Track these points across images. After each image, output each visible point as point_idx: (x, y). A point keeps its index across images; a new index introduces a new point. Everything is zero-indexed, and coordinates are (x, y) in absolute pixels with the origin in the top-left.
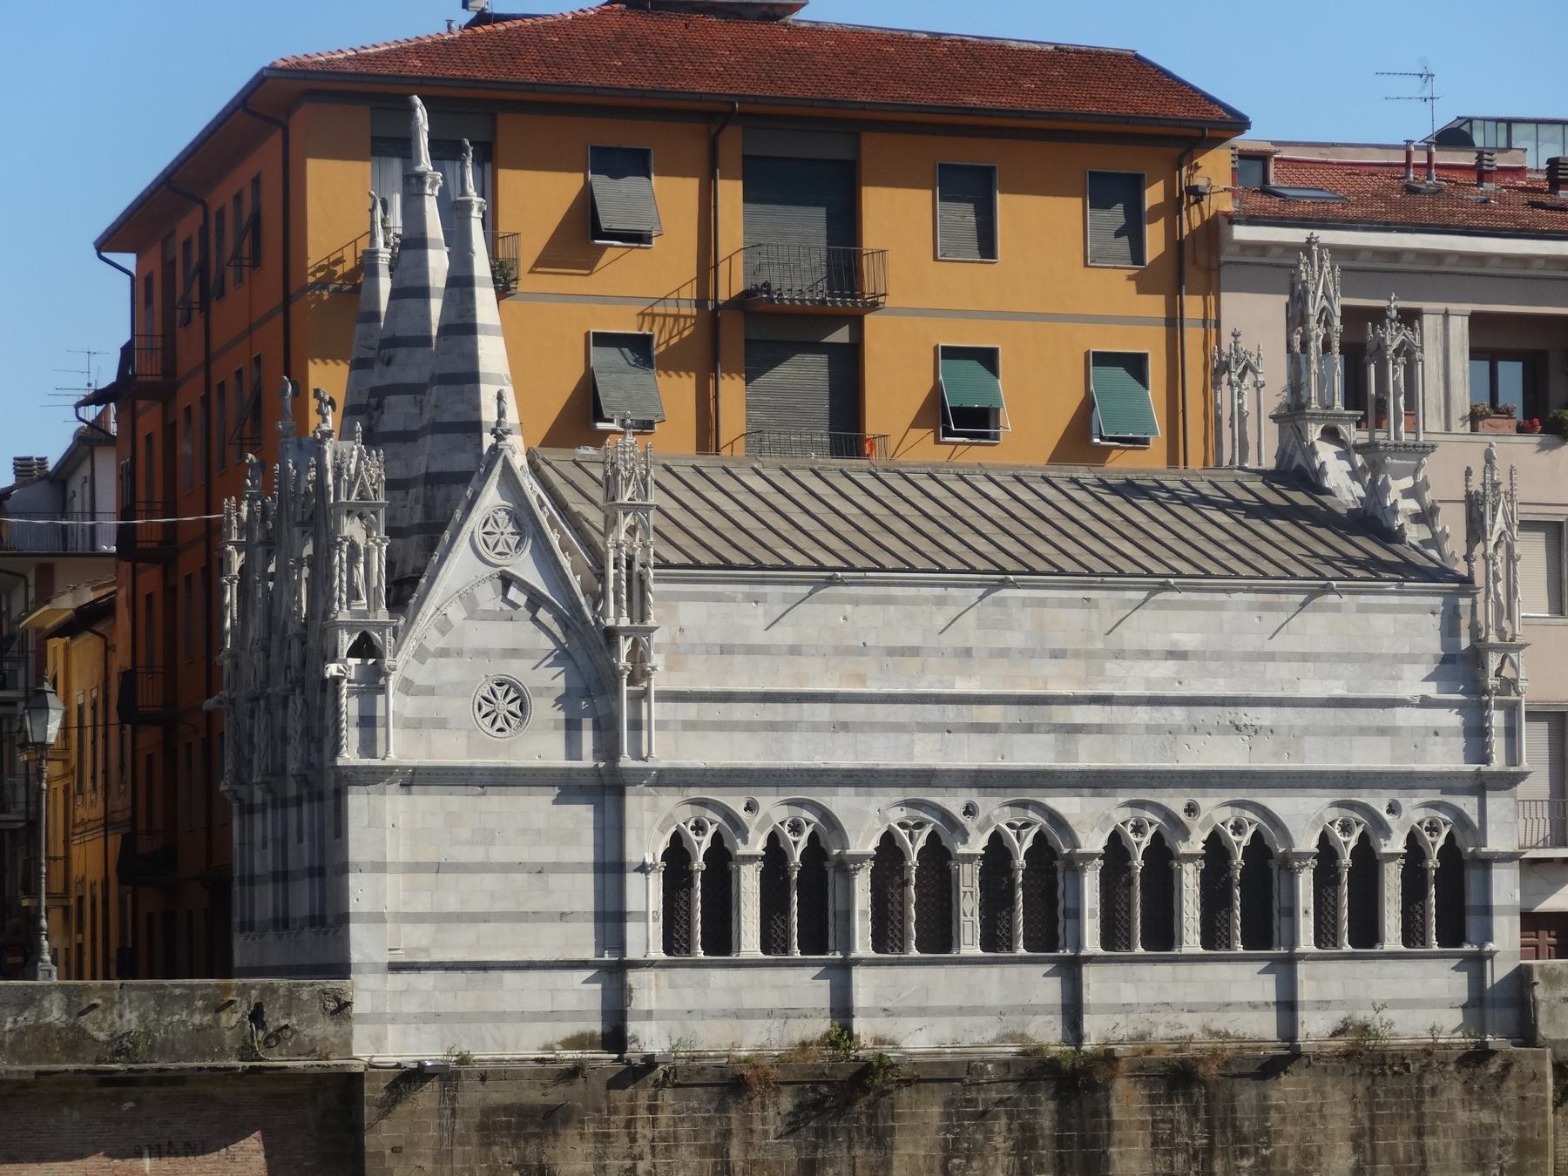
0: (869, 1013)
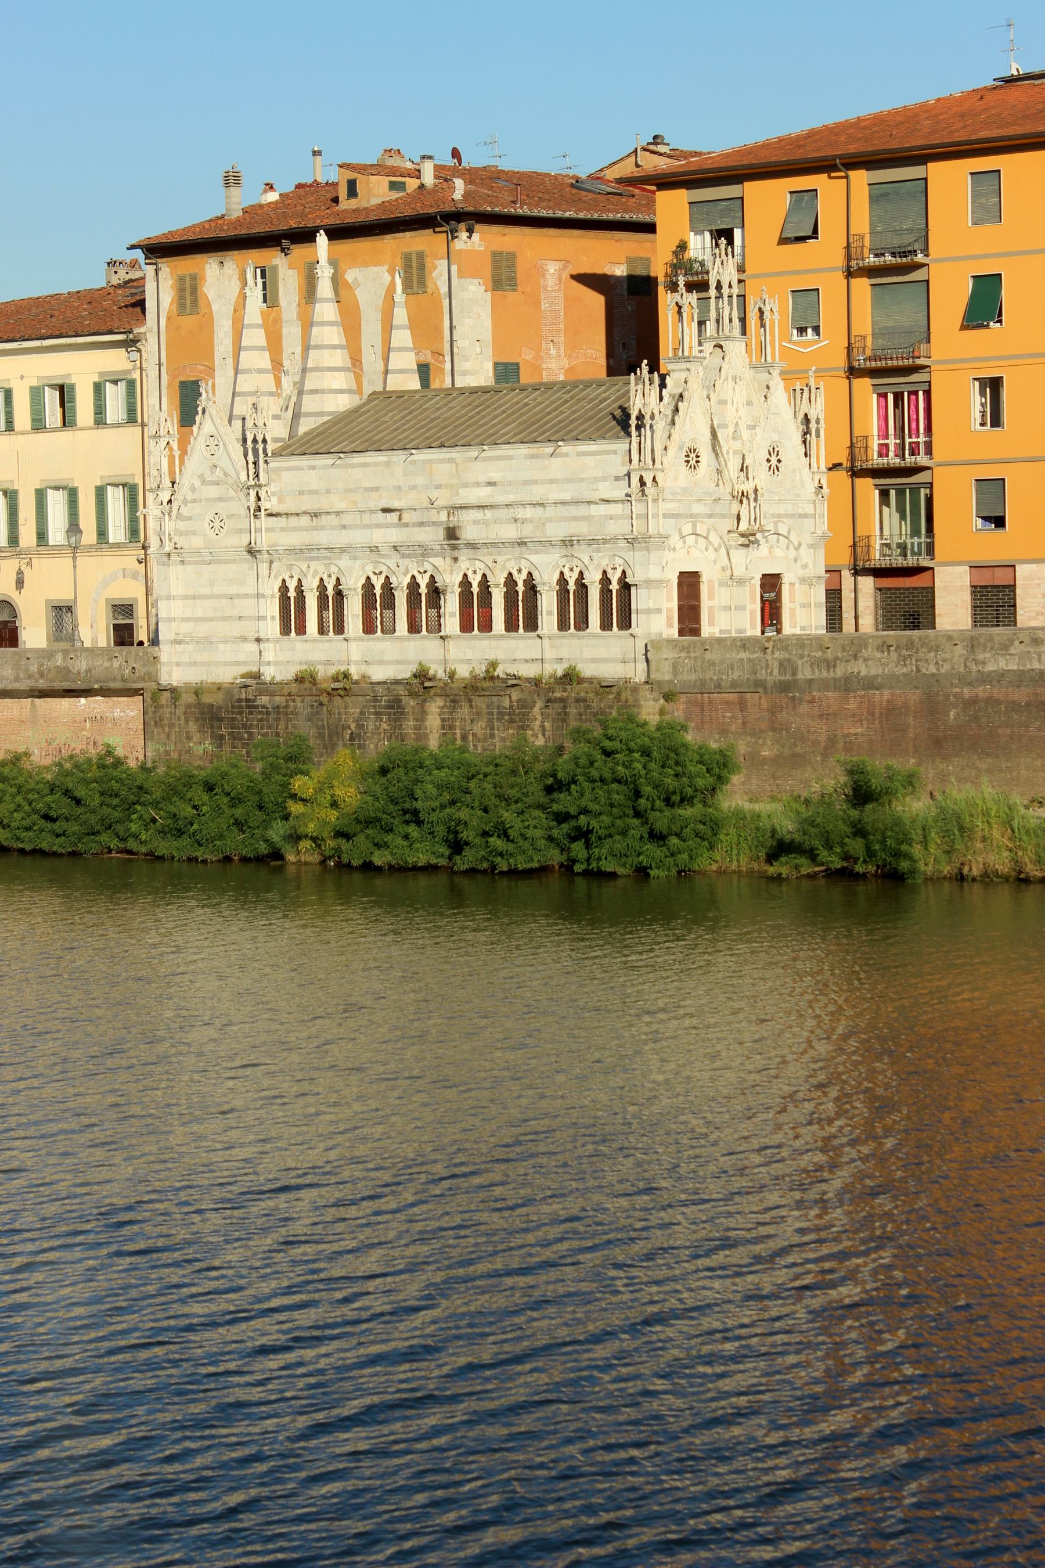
0: (356, 663)
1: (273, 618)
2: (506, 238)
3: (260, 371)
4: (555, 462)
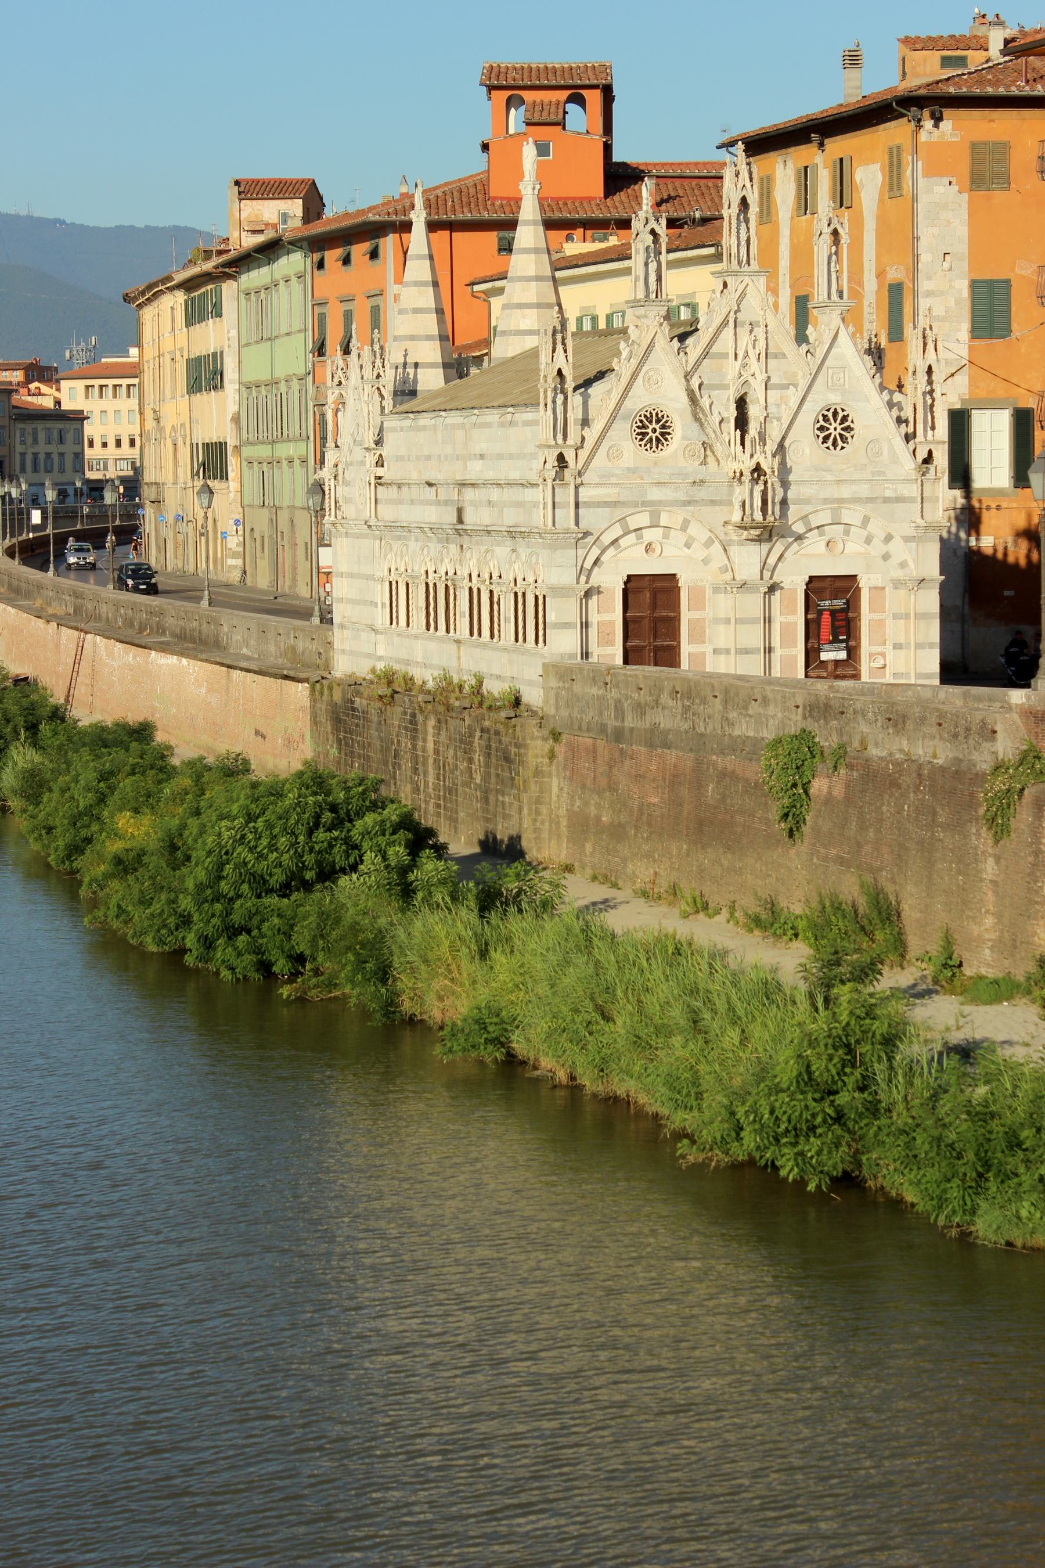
1: (383, 605)
2: (994, 125)
3: (417, 311)
4: (513, 430)
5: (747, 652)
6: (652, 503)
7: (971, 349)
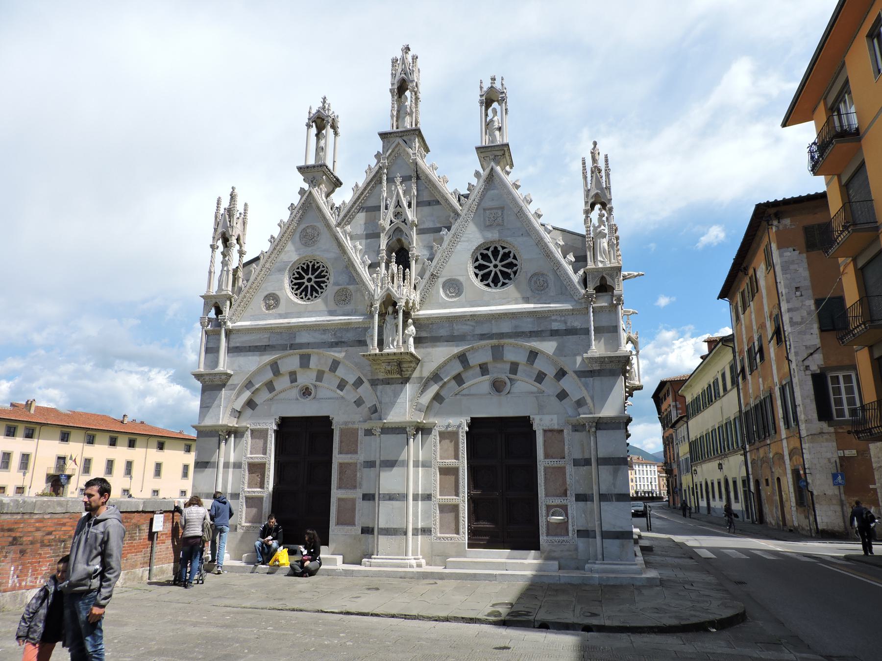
5: (391, 497)
6: (301, 346)
7: (822, 338)
